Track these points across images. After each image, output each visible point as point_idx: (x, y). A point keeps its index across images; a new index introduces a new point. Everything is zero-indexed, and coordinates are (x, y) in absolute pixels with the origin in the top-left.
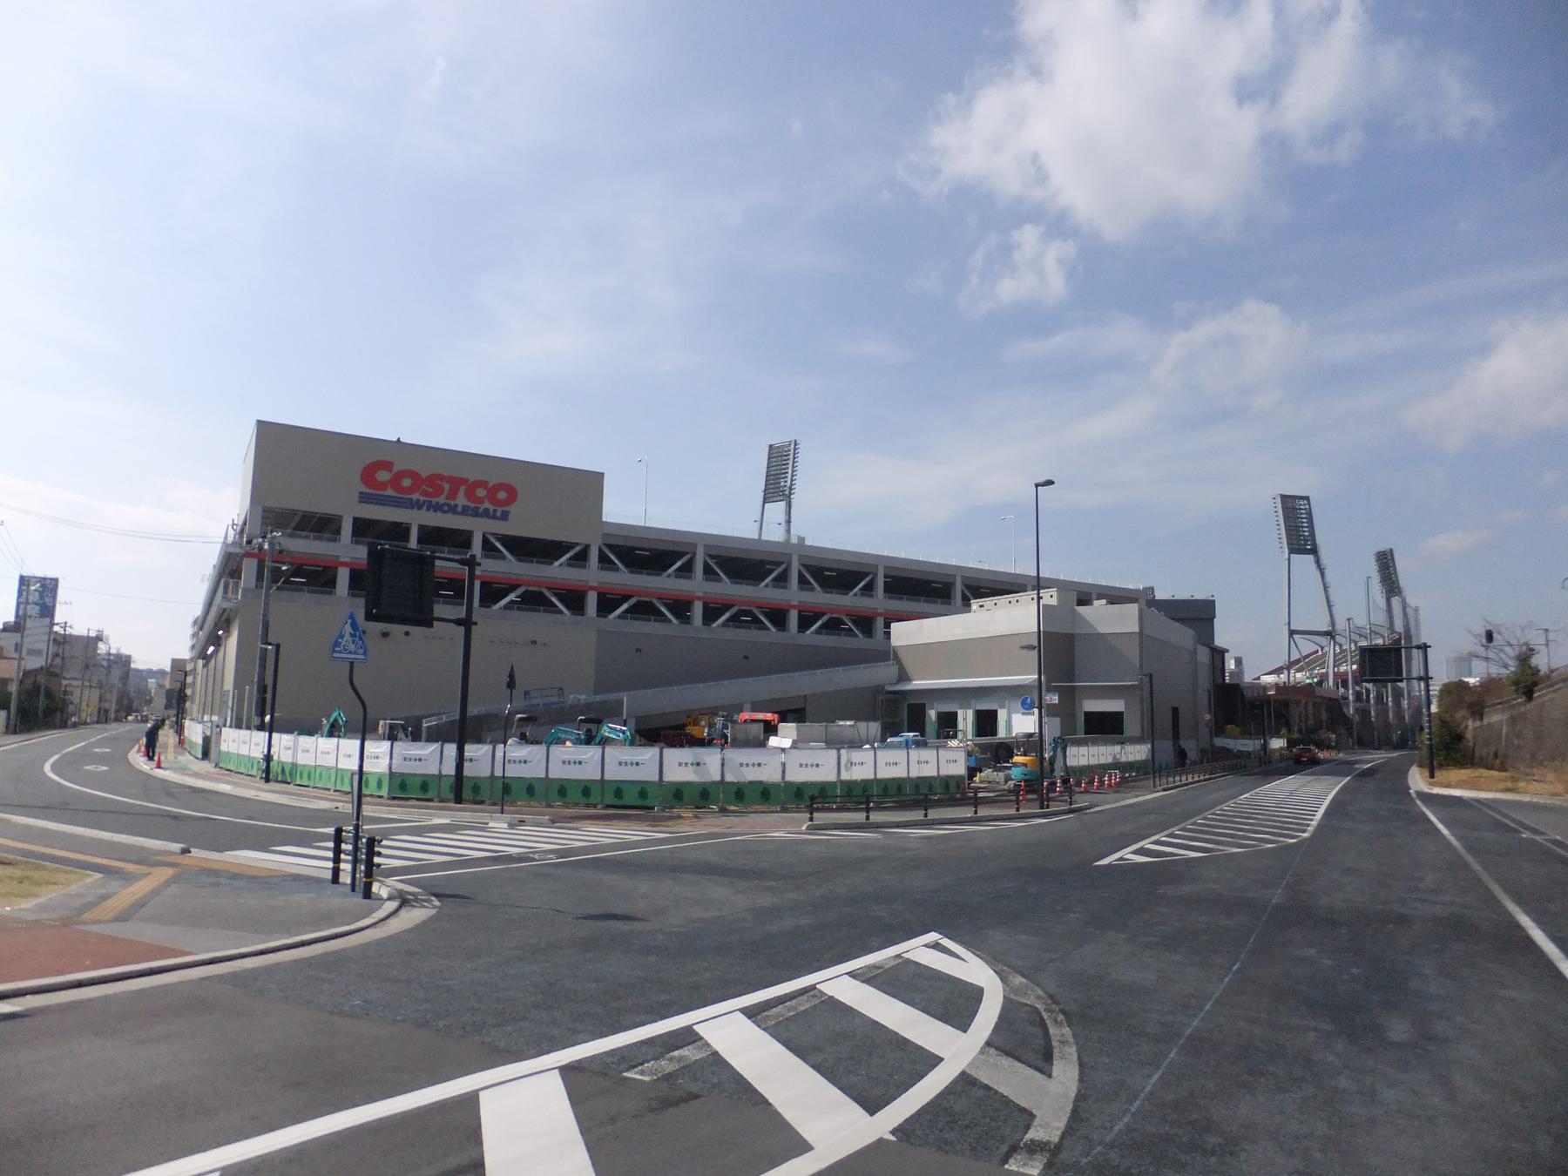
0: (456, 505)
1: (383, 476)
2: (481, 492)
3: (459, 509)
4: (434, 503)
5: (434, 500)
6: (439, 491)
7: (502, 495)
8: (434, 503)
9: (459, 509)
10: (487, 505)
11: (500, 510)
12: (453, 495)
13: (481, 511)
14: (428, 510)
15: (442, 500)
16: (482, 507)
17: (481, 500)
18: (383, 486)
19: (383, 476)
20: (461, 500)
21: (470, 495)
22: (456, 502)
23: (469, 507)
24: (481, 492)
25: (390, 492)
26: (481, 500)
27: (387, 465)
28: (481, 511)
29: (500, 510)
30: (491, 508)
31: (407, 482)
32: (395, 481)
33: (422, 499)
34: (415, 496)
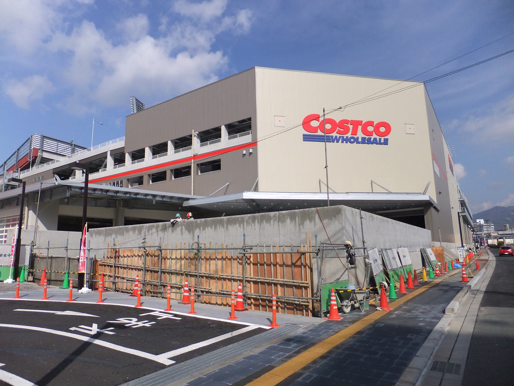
0: (358, 138)
1: (315, 124)
2: (370, 129)
3: (360, 140)
4: (345, 138)
5: (345, 136)
6: (347, 131)
7: (382, 129)
8: (345, 138)
9: (360, 140)
10: (374, 136)
11: (383, 138)
12: (355, 132)
13: (372, 140)
14: (342, 142)
15: (349, 135)
16: (372, 138)
17: (371, 134)
18: (315, 130)
19: (315, 124)
20: (360, 135)
21: (365, 131)
22: (357, 136)
23: (365, 138)
24: (370, 129)
25: (319, 133)
26: (371, 134)
27: (316, 117)
28: (372, 140)
29: (383, 138)
30: (378, 138)
31: (328, 126)
32: (322, 127)
33: (338, 135)
34: (334, 134)
